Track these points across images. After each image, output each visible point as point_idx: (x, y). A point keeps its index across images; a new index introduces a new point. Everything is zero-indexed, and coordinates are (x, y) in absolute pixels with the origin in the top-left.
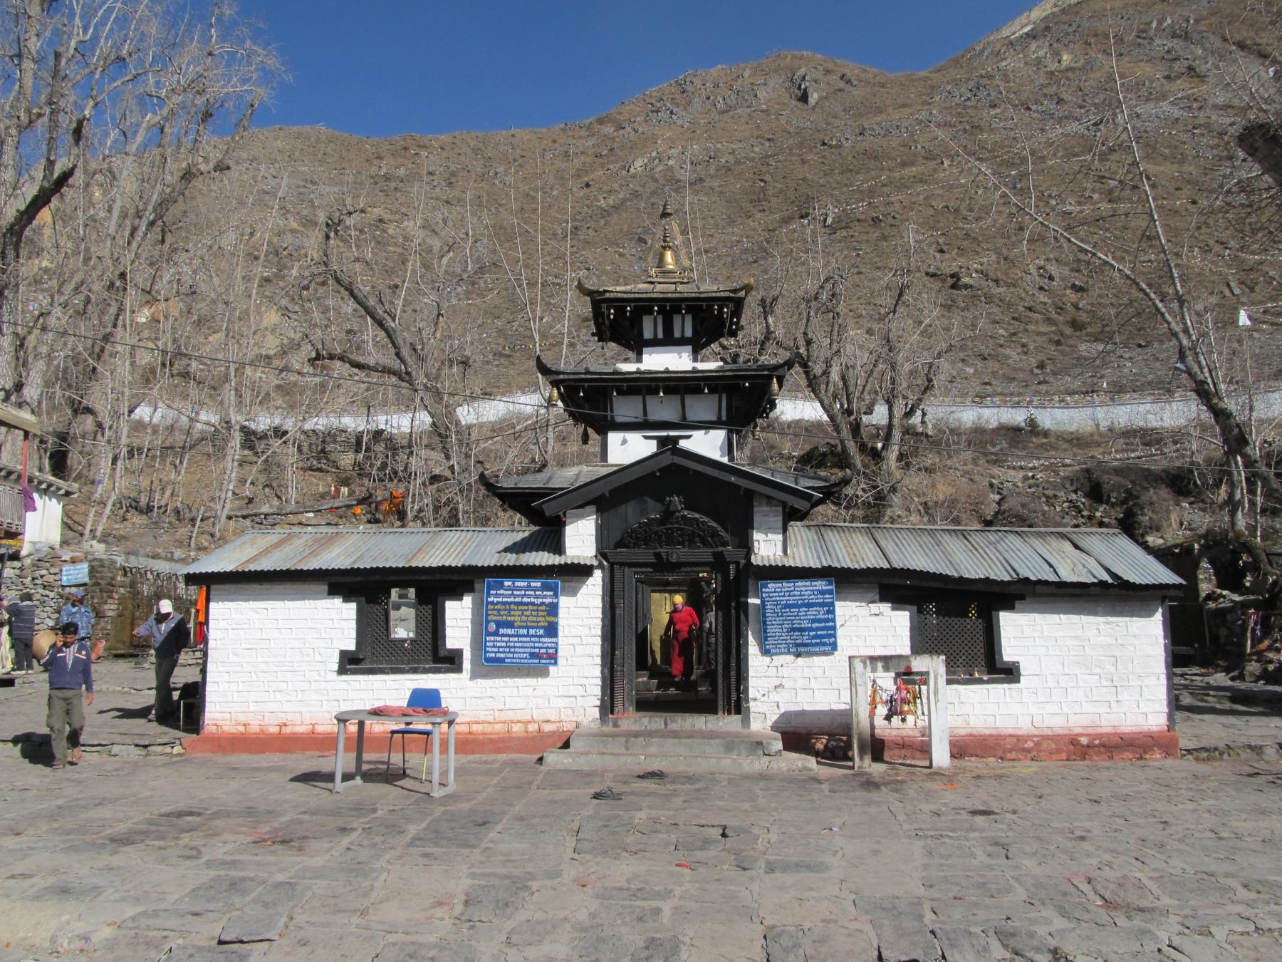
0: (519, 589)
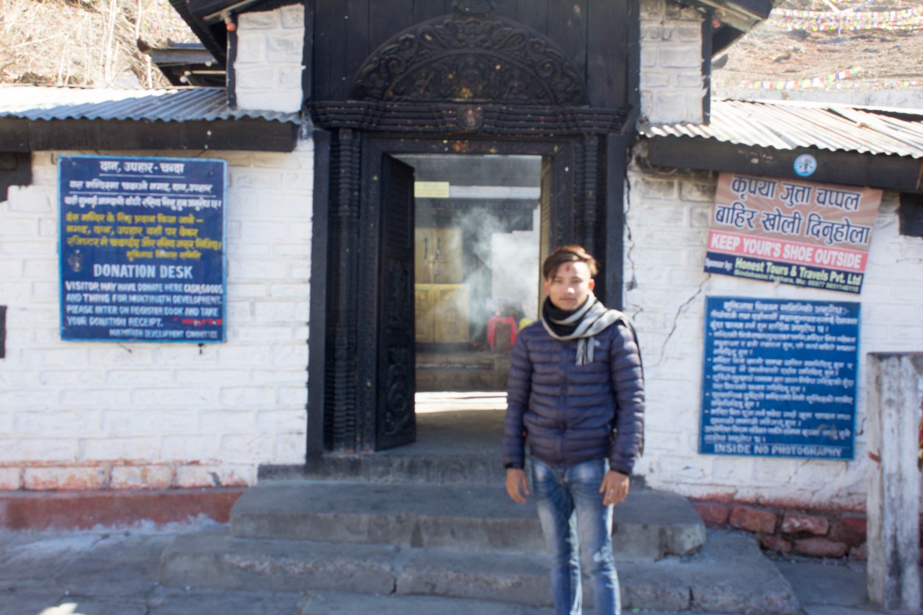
0: (137, 177)
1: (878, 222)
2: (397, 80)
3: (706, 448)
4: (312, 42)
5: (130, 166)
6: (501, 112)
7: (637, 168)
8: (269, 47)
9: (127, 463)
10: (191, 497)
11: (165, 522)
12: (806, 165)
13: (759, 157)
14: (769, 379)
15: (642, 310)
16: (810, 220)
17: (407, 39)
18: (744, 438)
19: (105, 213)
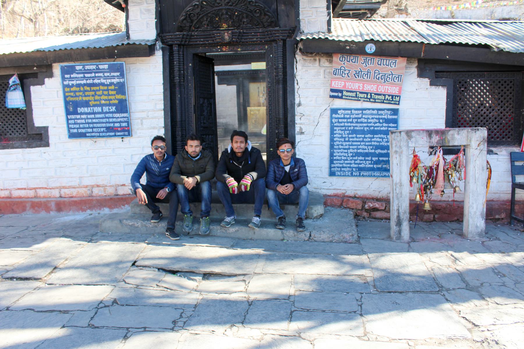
0: (90, 72)
1: (408, 72)
2: (194, 23)
3: (332, 174)
4: (159, 9)
5: (87, 67)
6: (240, 33)
7: (300, 54)
8: (141, 12)
9: (98, 186)
10: (122, 199)
11: (113, 208)
12: (370, 48)
13: (349, 46)
14: (359, 143)
15: (304, 115)
16: (375, 73)
17: (196, 5)
18: (348, 169)
19: (80, 87)
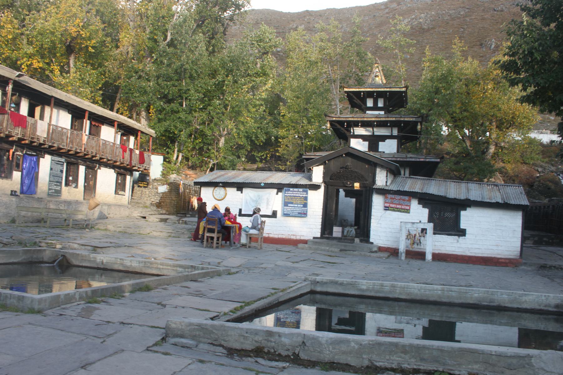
0: (295, 191)
